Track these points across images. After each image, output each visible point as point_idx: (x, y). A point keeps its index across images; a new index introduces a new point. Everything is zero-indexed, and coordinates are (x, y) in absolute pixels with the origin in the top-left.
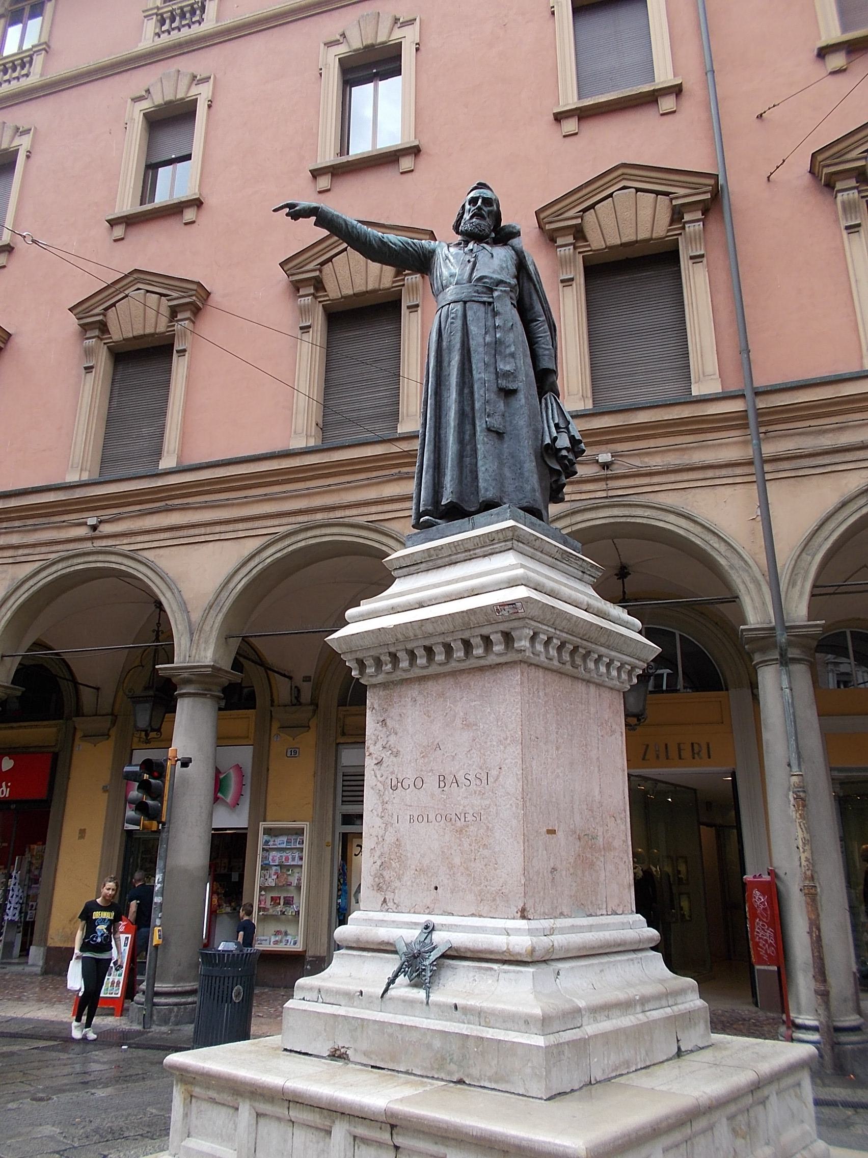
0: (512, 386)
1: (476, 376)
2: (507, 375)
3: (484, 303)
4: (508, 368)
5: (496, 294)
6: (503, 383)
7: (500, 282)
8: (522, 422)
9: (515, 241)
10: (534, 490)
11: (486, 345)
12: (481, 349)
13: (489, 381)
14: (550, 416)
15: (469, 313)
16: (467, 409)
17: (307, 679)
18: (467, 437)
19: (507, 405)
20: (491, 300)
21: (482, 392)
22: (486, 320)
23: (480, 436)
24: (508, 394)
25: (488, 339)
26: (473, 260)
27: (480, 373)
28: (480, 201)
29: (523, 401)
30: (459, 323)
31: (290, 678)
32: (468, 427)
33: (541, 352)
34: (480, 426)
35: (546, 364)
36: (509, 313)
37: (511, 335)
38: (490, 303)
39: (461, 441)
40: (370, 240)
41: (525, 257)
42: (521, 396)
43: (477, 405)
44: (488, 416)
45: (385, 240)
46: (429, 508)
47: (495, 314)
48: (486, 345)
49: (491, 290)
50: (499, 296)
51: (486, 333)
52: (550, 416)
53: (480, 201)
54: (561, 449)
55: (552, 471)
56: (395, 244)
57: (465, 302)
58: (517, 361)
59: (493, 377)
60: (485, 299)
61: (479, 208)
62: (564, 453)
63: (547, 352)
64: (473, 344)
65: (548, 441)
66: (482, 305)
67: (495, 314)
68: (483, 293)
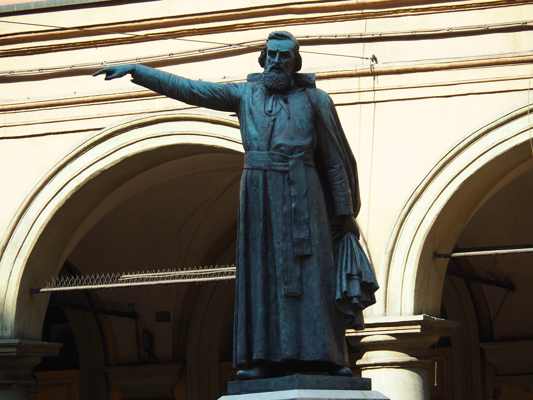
0: (307, 252)
1: (277, 246)
2: (300, 242)
3: (281, 172)
4: (302, 236)
5: (291, 163)
6: (298, 251)
7: (293, 150)
8: (313, 283)
9: (310, 91)
10: (324, 346)
11: (285, 215)
12: (280, 219)
13: (286, 250)
14: (344, 266)
15: (269, 183)
16: (271, 270)
17: (163, 317)
18: (272, 296)
19: (302, 267)
20: (287, 168)
21: (281, 261)
22: (284, 190)
23: (281, 302)
24: (302, 259)
25: (285, 209)
26: (272, 123)
27: (278, 244)
28: (278, 54)
29: (315, 265)
30: (261, 192)
31: (134, 315)
32: (272, 287)
33: (338, 198)
34: (282, 290)
35: (342, 211)
36: (306, 178)
37: (305, 202)
38: (287, 172)
39: (267, 304)
40: (181, 93)
41: (320, 111)
42: (314, 259)
43: (278, 272)
44: (286, 285)
45: (195, 91)
46: (244, 361)
47: (291, 183)
48: (285, 215)
49: (285, 159)
50: (294, 166)
51: (284, 203)
52: (344, 266)
53: (278, 54)
54: (352, 297)
55: (347, 316)
56: (204, 94)
57: (265, 171)
58: (311, 226)
59: (290, 245)
60: (282, 168)
61: (277, 64)
62: (355, 301)
63: (343, 199)
64: (273, 214)
65: (338, 296)
66: (279, 174)
67: (291, 183)
68: (280, 161)
